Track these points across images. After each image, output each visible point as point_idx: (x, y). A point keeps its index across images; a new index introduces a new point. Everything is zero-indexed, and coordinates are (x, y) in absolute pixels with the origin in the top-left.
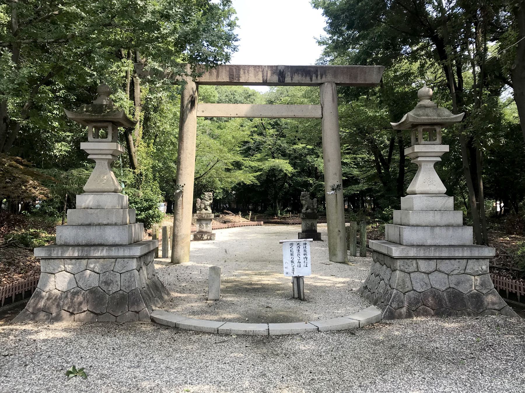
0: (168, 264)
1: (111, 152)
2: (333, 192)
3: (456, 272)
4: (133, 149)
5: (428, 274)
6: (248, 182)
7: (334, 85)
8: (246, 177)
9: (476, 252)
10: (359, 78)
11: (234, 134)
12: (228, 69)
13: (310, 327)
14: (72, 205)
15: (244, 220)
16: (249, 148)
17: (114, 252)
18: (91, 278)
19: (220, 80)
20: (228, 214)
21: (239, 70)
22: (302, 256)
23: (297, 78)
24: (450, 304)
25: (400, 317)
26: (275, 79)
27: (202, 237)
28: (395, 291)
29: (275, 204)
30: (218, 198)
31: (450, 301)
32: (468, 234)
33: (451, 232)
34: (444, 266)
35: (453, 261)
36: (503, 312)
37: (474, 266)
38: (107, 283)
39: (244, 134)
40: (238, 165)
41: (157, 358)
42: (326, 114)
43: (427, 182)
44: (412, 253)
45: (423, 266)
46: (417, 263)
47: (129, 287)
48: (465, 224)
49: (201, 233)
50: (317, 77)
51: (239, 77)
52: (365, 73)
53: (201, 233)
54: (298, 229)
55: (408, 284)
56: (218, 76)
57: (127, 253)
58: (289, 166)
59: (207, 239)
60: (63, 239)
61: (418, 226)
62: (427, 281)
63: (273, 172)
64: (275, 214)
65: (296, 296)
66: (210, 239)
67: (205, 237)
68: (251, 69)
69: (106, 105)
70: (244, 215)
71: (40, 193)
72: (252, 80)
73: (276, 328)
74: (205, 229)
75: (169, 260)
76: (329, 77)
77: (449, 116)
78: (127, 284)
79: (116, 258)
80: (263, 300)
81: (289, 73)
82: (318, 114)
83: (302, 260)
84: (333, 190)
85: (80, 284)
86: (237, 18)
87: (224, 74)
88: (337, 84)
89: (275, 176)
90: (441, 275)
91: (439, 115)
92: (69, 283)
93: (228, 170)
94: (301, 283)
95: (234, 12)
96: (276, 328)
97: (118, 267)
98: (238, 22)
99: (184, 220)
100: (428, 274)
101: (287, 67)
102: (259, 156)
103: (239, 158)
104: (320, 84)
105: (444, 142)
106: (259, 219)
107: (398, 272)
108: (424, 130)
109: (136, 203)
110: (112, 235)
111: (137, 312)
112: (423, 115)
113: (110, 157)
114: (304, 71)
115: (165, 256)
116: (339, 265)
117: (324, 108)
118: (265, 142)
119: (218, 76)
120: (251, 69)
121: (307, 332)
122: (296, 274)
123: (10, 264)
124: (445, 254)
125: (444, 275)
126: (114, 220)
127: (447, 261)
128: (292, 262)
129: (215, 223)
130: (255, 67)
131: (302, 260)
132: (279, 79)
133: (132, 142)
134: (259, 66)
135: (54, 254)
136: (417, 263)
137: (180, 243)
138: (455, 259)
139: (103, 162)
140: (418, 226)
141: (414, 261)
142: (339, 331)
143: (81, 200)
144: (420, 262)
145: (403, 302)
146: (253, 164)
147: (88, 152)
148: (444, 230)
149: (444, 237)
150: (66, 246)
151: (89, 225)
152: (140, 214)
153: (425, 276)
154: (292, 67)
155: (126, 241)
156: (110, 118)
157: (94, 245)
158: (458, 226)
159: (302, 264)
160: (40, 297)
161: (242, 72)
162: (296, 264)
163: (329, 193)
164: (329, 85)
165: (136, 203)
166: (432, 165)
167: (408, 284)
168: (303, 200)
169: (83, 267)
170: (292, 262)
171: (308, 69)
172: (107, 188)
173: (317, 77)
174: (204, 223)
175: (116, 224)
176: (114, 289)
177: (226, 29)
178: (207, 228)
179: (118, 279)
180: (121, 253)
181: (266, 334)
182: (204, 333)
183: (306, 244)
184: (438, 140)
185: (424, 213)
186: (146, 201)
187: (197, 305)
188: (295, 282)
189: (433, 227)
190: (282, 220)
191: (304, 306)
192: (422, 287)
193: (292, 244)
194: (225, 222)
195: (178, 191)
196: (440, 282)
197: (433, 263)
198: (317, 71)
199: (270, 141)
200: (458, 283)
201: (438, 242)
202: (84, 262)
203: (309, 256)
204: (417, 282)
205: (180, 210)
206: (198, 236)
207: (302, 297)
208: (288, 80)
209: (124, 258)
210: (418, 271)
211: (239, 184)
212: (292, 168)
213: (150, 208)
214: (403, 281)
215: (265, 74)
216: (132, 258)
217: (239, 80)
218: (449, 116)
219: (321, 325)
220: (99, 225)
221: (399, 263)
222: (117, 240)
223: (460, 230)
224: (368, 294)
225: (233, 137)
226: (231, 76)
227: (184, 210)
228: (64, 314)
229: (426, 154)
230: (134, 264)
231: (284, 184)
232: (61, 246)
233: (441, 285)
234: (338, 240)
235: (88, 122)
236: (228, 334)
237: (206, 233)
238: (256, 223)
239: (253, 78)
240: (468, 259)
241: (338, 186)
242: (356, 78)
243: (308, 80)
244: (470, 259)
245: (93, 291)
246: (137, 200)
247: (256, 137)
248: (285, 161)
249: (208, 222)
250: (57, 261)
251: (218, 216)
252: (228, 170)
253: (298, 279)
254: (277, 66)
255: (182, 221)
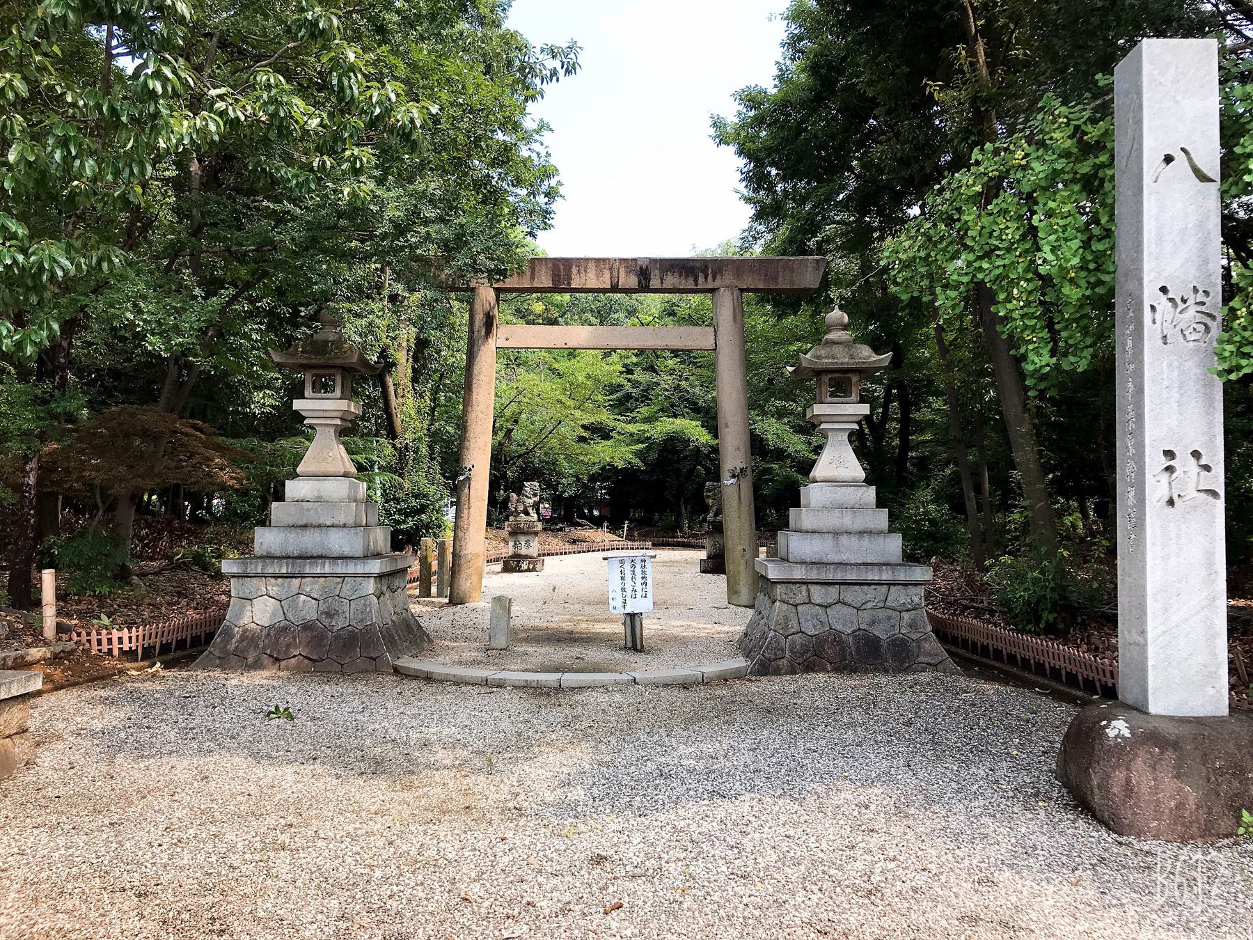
0: (442, 606)
1: (339, 414)
2: (732, 481)
3: (870, 605)
4: (394, 402)
5: (826, 607)
6: (621, 465)
7: (736, 293)
8: (616, 453)
9: (902, 576)
10: (780, 279)
11: (590, 370)
12: (550, 265)
13: (625, 677)
14: (280, 497)
15: (615, 537)
16: (628, 397)
17: (340, 568)
18: (308, 609)
19: (536, 284)
20: (582, 525)
21: (570, 267)
22: (639, 581)
23: (671, 280)
24: (862, 655)
25: (777, 672)
26: (633, 281)
27: (518, 565)
28: (772, 634)
29: (679, 506)
30: (566, 495)
31: (858, 649)
32: (894, 545)
33: (866, 542)
34: (851, 595)
35: (865, 587)
36: (941, 667)
37: (898, 597)
38: (329, 615)
39: (612, 370)
40: (602, 432)
41: (390, 705)
42: (722, 342)
43: (839, 463)
44: (799, 573)
45: (818, 594)
46: (808, 591)
47: (362, 620)
48: (891, 530)
49: (517, 557)
50: (706, 278)
51: (569, 279)
52: (792, 270)
53: (517, 557)
54: (703, 555)
55: (794, 623)
56: (532, 278)
57: (360, 568)
58: (704, 431)
59: (528, 570)
60: (264, 547)
61: (814, 532)
62: (823, 618)
63: (673, 446)
64: (677, 526)
65: (630, 644)
66: (534, 570)
67: (525, 566)
68: (591, 265)
69: (333, 342)
70: (615, 528)
71: (232, 478)
72: (592, 283)
73: (570, 679)
74: (523, 552)
75: (446, 600)
76: (728, 278)
77: (869, 357)
78: (360, 617)
79: (343, 577)
80: (576, 651)
81: (657, 272)
82: (710, 343)
83: (638, 587)
84: (734, 476)
85: (289, 615)
86: (559, 183)
87: (543, 273)
88: (742, 290)
89: (674, 451)
90: (846, 610)
91: (852, 357)
92: (274, 615)
93: (582, 439)
94: (637, 623)
95: (556, 172)
96: (570, 679)
97: (347, 589)
98: (562, 190)
99: (471, 528)
100: (826, 607)
101: (654, 261)
102: (645, 411)
103: (605, 417)
104: (713, 291)
105: (862, 400)
106: (643, 537)
107: (778, 603)
108: (830, 379)
109: (397, 500)
110: (338, 542)
111: (375, 659)
112: (827, 357)
113: (338, 422)
114: (683, 268)
115: (440, 595)
116: (741, 609)
117: (721, 334)
118: (658, 384)
119: (532, 278)
120: (591, 265)
121: (617, 683)
122: (629, 610)
123: (180, 595)
124: (852, 576)
125: (850, 610)
126: (341, 519)
127: (856, 587)
128: (623, 590)
129: (555, 543)
130: (597, 261)
131: (638, 587)
132: (640, 282)
133: (392, 389)
134: (604, 260)
135: (251, 570)
136: (808, 591)
137: (463, 568)
138: (869, 584)
139: (327, 429)
140: (814, 532)
141: (804, 587)
142: (667, 685)
143: (293, 488)
144: (813, 588)
145: (783, 650)
146: (631, 428)
147: (303, 414)
148: (854, 540)
149: (854, 551)
150: (269, 557)
151: (305, 526)
152: (404, 522)
153: (820, 610)
154: (662, 261)
155: (359, 553)
156: (339, 362)
157: (312, 557)
158: (880, 533)
159: (639, 594)
160: (228, 634)
161: (574, 270)
162: (629, 593)
163: (728, 481)
164: (728, 293)
165: (397, 500)
166: (845, 437)
167: (794, 623)
168: (708, 497)
169: (295, 591)
170: (623, 590)
171: (691, 264)
172: (331, 469)
173: (706, 278)
174: (523, 539)
175: (344, 526)
176: (339, 623)
177: (542, 199)
178: (533, 547)
179: (346, 608)
180: (351, 568)
181: (557, 685)
182: (467, 684)
183: (644, 561)
184: (854, 397)
185: (825, 513)
186: (416, 496)
187: (467, 656)
188: (628, 622)
189: (836, 534)
190: (691, 540)
191: (638, 658)
192: (815, 627)
193: (622, 562)
194: (574, 542)
195: (462, 478)
196: (843, 621)
197: (833, 590)
198: (706, 267)
199: (666, 381)
200: (873, 622)
201: (845, 557)
202: (296, 582)
203: (649, 581)
204: (807, 621)
205: (465, 511)
206: (512, 565)
207: (639, 647)
208: (655, 283)
209: (355, 576)
210: (810, 602)
211: (603, 468)
212: (709, 437)
213: (423, 509)
214: (786, 619)
215: (615, 274)
216: (367, 576)
217: (569, 284)
218: (869, 357)
219: (638, 676)
220: (319, 526)
221: (779, 590)
222: (347, 550)
223: (881, 539)
224: (745, 645)
225: (589, 377)
226: (556, 277)
227: (472, 511)
228: (266, 660)
229: (832, 418)
230: (370, 586)
231: (695, 466)
232: (262, 557)
233: (844, 625)
234: (742, 567)
235: (304, 368)
236: (501, 685)
237: (526, 557)
238: (638, 544)
239: (594, 281)
240: (890, 584)
241: (741, 470)
242: (775, 279)
243: (690, 284)
244: (894, 584)
245: (307, 627)
246: (400, 495)
247: (639, 375)
248: (694, 423)
249: (530, 537)
250: (255, 581)
251: (561, 529)
252: (582, 439)
253: (633, 619)
254: (635, 260)
255: (467, 529)
